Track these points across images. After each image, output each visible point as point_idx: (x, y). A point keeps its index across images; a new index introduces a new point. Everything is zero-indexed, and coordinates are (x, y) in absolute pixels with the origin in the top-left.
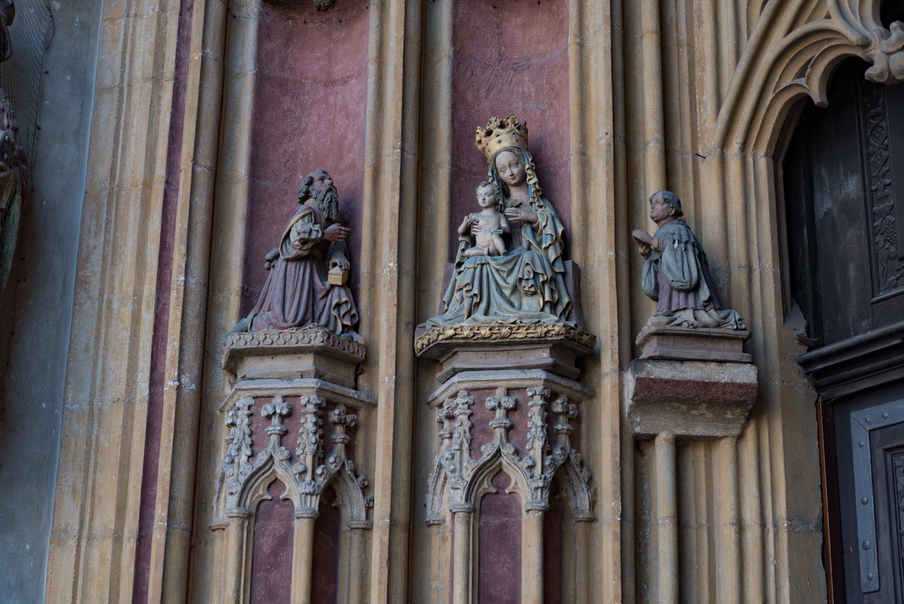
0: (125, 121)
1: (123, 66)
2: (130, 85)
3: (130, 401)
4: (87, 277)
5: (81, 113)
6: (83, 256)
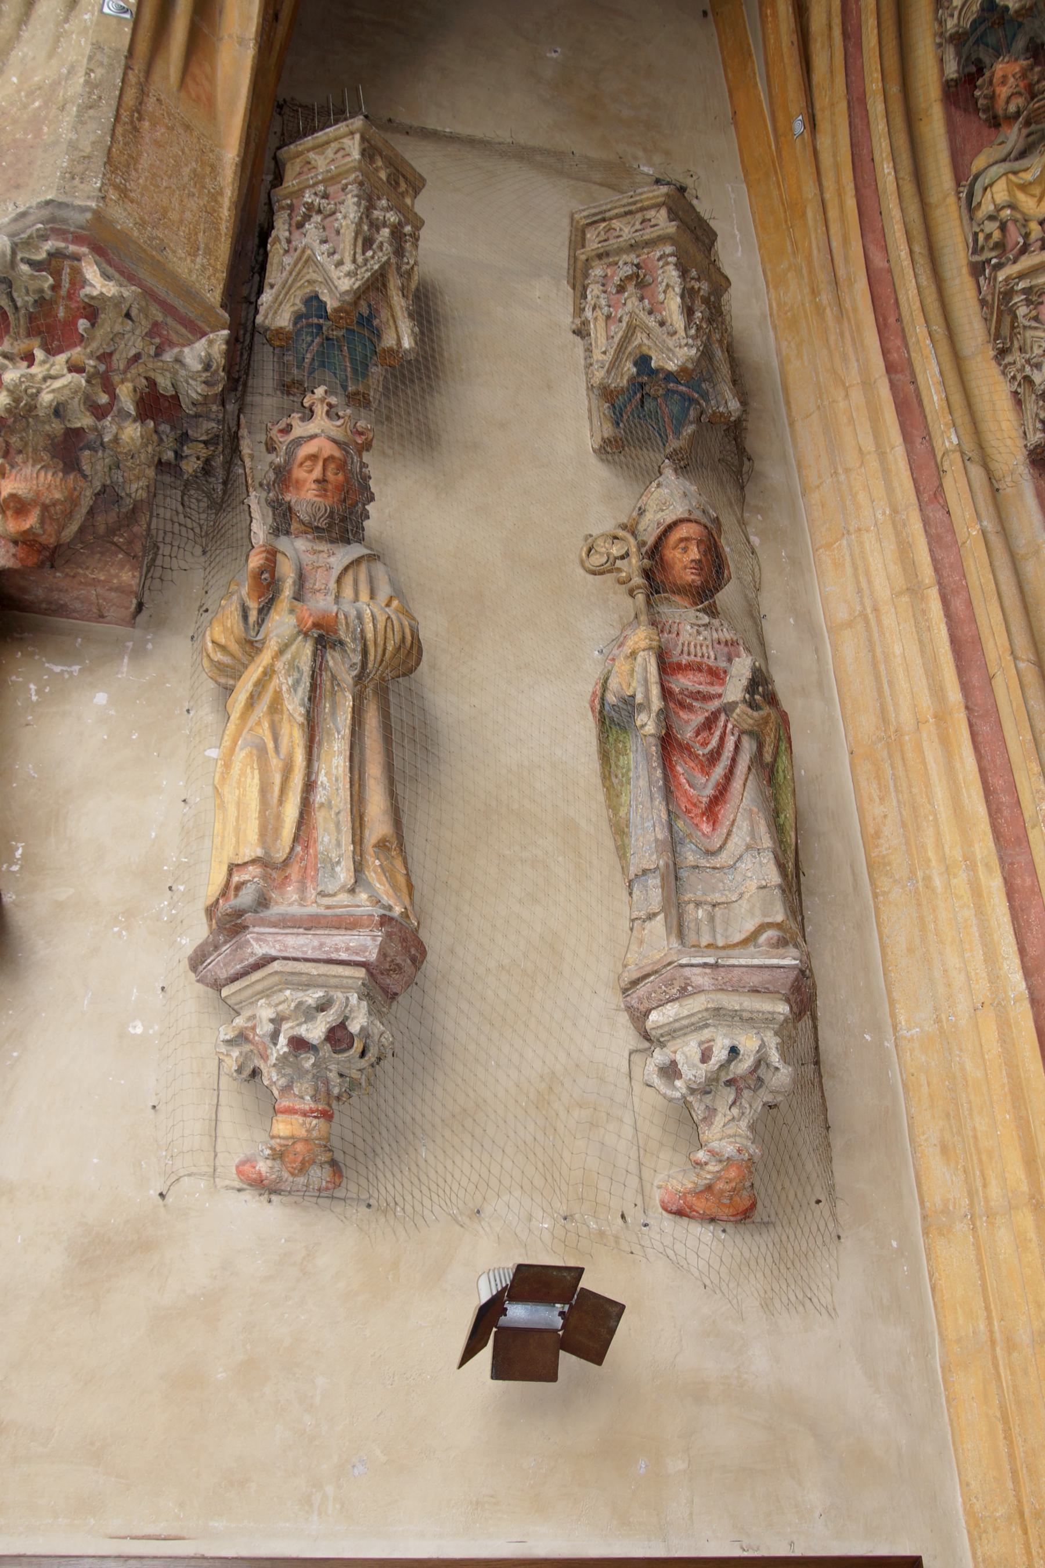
0: (884, 652)
1: (860, 591)
2: (876, 610)
3: (999, 1004)
4: (884, 857)
5: (818, 660)
6: (871, 830)
